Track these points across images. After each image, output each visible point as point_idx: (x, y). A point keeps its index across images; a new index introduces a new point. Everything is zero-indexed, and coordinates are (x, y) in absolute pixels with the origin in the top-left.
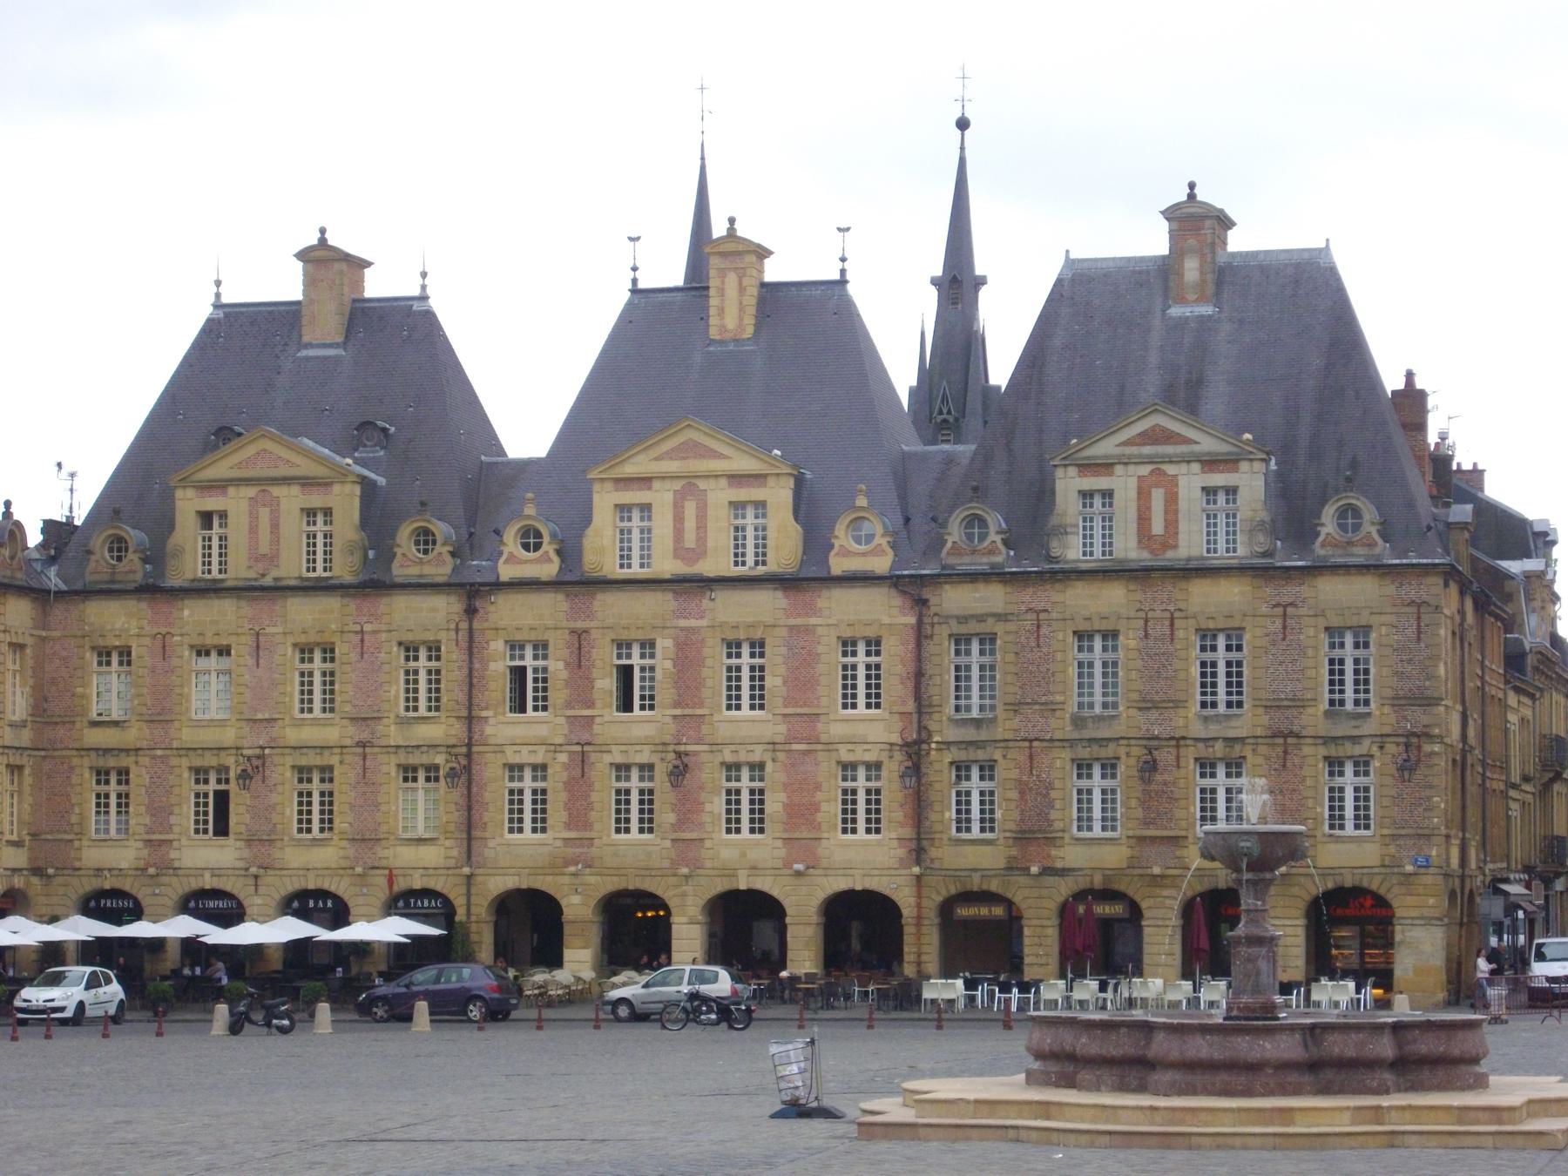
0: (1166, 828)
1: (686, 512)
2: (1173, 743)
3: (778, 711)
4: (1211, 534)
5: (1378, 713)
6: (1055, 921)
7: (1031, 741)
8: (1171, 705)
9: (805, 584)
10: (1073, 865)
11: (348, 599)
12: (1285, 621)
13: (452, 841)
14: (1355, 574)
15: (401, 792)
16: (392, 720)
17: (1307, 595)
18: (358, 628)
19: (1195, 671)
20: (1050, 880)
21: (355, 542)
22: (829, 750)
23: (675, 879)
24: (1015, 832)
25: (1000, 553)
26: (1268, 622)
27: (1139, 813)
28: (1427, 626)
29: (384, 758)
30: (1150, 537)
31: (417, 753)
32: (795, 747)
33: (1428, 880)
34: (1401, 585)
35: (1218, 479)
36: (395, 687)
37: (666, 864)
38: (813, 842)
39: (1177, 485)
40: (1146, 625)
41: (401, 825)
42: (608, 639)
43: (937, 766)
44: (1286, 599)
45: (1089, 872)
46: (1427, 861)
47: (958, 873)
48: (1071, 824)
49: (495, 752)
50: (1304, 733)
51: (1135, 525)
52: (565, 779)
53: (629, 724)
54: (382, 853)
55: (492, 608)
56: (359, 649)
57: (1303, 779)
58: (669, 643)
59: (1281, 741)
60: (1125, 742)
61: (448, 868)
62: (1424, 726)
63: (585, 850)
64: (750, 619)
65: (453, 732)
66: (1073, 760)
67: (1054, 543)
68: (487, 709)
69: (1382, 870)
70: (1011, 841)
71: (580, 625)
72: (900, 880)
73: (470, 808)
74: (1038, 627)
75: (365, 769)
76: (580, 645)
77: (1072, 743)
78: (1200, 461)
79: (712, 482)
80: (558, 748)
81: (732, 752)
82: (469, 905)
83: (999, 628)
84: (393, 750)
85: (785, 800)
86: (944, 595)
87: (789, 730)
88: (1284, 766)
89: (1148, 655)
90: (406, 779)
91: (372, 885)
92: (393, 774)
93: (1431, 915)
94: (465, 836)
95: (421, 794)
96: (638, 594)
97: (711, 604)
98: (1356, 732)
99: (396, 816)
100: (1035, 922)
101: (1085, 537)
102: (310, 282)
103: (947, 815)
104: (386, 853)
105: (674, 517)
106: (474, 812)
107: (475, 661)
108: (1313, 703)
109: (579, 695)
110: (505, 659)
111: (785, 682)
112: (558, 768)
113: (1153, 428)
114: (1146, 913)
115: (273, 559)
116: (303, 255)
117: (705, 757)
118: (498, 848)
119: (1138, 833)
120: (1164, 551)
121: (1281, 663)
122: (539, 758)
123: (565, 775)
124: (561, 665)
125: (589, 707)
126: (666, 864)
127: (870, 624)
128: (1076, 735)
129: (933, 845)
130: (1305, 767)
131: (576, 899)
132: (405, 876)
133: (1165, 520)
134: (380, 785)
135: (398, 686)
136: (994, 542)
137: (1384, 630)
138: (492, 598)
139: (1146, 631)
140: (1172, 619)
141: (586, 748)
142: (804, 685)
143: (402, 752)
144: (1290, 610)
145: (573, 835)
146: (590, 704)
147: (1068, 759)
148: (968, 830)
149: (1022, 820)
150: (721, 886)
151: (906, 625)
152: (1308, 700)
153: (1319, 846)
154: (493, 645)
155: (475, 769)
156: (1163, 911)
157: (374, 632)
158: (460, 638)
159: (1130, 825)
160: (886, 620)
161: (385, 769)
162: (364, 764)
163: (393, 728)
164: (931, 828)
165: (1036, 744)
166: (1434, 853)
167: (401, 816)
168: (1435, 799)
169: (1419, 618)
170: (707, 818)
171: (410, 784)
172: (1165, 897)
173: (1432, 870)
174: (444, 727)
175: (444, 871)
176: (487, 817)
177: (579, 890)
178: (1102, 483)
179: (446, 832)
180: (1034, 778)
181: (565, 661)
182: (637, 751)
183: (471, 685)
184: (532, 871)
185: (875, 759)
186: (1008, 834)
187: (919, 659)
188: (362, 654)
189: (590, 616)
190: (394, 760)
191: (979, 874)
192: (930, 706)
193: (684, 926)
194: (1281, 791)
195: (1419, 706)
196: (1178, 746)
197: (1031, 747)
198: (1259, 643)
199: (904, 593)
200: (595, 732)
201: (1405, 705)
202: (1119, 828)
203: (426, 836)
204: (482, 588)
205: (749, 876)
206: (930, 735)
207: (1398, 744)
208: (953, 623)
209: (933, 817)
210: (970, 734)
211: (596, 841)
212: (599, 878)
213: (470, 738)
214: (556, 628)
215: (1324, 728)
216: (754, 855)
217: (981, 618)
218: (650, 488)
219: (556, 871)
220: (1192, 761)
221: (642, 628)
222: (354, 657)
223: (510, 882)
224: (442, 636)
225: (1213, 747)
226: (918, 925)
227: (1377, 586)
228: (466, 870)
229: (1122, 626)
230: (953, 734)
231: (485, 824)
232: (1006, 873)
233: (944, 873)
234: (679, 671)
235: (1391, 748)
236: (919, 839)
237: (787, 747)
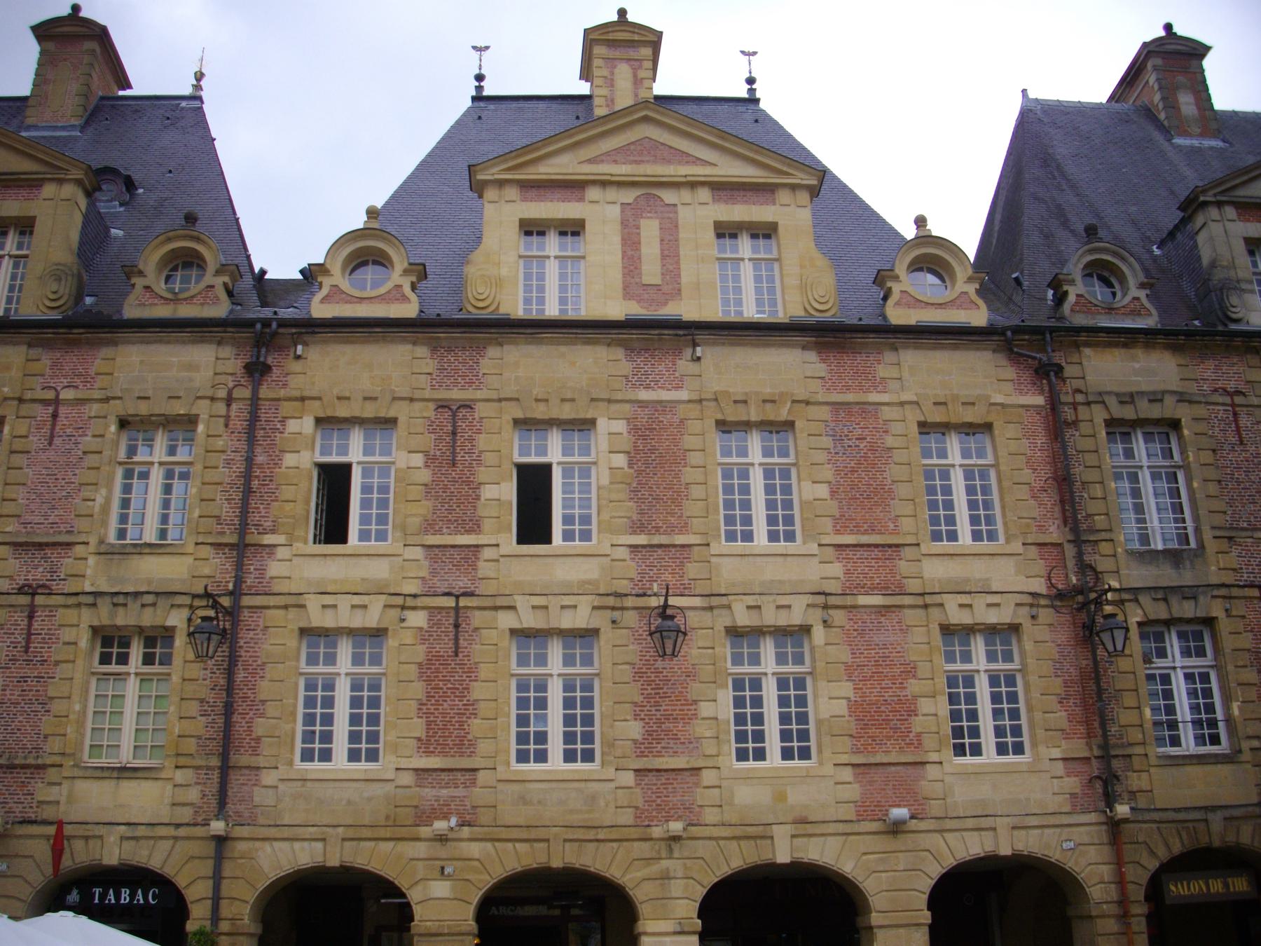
1: (643, 234)
3: (826, 540)
9: (859, 339)
11: (40, 350)
13: (190, 772)
15: (94, 682)
16: (92, 548)
18: (50, 395)
21: (64, 265)
22: (926, 606)
23: (646, 845)
29: (70, 615)
31: (134, 606)
32: (863, 600)
36: (104, 492)
37: (627, 817)
38: (910, 770)
41: (88, 742)
42: (507, 418)
47: (1181, 816)
49: (286, 607)
52: (421, 658)
53: (550, 560)
54: (43, 792)
55: (296, 366)
56: (46, 430)
58: (620, 426)
61: (178, 826)
63: (460, 792)
64: (768, 391)
65: (207, 571)
68: (273, 532)
71: (456, 394)
72: (1081, 834)
73: (229, 710)
74: (1235, 414)
75: (29, 634)
76: (454, 426)
79: (686, 195)
80: (410, 602)
81: (749, 607)
82: (216, 899)
84: (90, 599)
85: (851, 694)
87: (847, 572)
90: (105, 660)
91: (16, 856)
92: (84, 643)
94: (215, 762)
95: (132, 688)
96: (563, 349)
97: (693, 368)
99: (81, 723)
104: (53, 793)
105: (623, 239)
106: (236, 718)
107: (258, 450)
109: (450, 511)
110: (313, 450)
111: (833, 493)
112: (408, 638)
117: (693, 619)
118: (282, 787)
122: (371, 619)
123: (420, 653)
124: (418, 460)
125: (469, 532)
126: (627, 817)
127: (973, 404)
131: (441, 889)
132: (87, 838)
134: (57, 663)
135: (110, 492)
136: (1137, 299)
138: (300, 348)
141: (463, 602)
142: (869, 498)
143: (104, 606)
145: (434, 762)
146: (474, 526)
150: (736, 859)
154: (292, 426)
155: (244, 637)
158: (233, 414)
160: (999, 398)
161: (68, 634)
162: (30, 625)
163: (92, 560)
164: (1121, 737)
167: (89, 725)
170: (702, 729)
171: (114, 668)
174: (190, 560)
175: (171, 831)
176: (261, 727)
177: (448, 870)
179: (178, 755)
181: (426, 453)
182: (563, 607)
183: (248, 491)
184: (351, 833)
185: (1008, 621)
188: (52, 437)
189: (474, 380)
190: (87, 618)
193: (667, 939)
200: (480, 574)
203: (139, 763)
204: (281, 330)
205: (793, 836)
208: (1112, 402)
210: (1166, 575)
211: (481, 774)
212: (489, 845)
213: (239, 581)
214: (412, 400)
216: (797, 797)
218: (581, 199)
219: (403, 832)
221: (573, 400)
222: (35, 441)
223: (305, 855)
224: (202, 408)
228: (218, 827)
230: (1137, 575)
231: (258, 740)
233: (1156, 816)
234: (639, 472)
237: (849, 601)
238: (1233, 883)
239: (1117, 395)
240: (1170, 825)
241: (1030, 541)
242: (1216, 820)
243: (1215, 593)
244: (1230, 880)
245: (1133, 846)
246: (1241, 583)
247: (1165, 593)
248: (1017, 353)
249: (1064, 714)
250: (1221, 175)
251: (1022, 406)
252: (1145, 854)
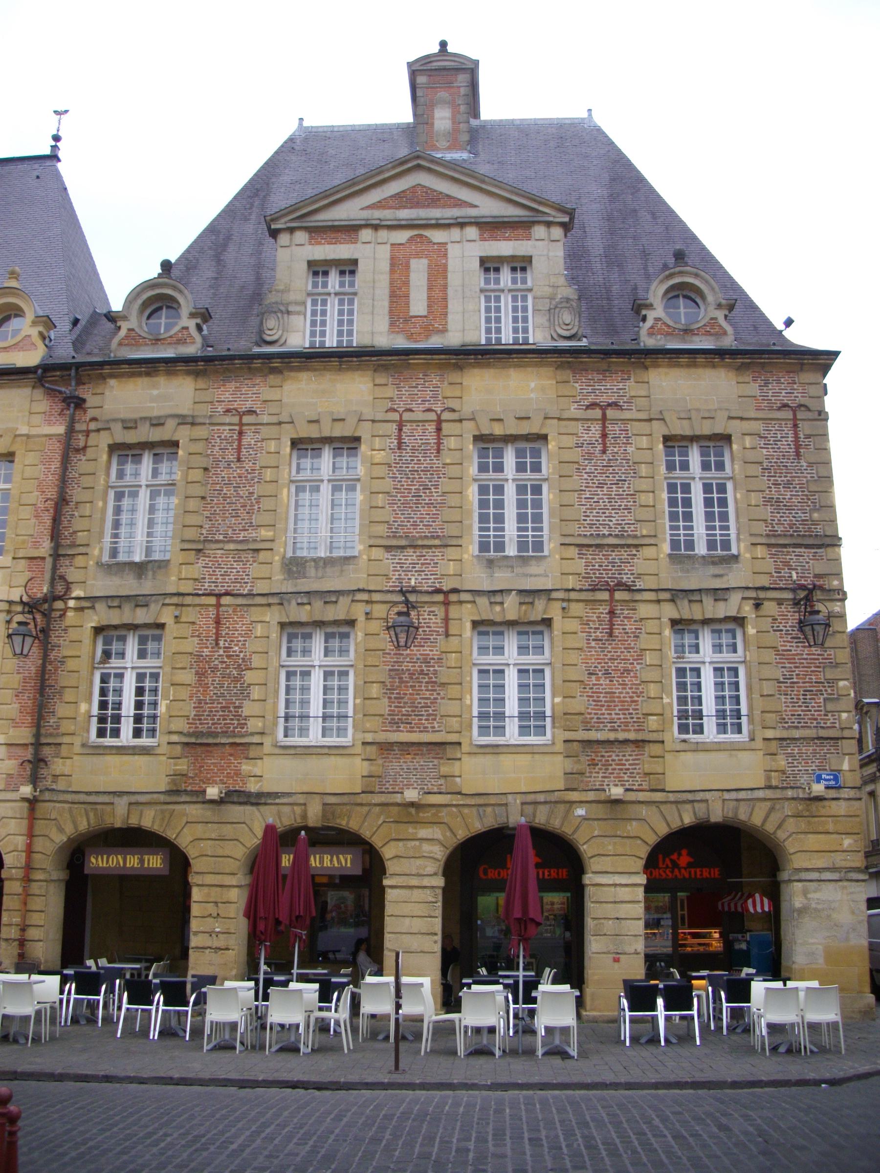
0: (425, 730)
2: (440, 598)
5: (748, 555)
6: (242, 879)
7: (219, 596)
8: (437, 542)
10: (275, 789)
12: (604, 427)
14: (704, 366)
17: (633, 394)
19: (472, 493)
20: (236, 811)
24: (189, 735)
25: (193, 343)
26: (579, 427)
27: (383, 706)
28: (808, 436)
30: (408, 319)
33: (841, 808)
34: (766, 384)
35: (504, 248)
39: (445, 255)
40: (400, 430)
43: (73, 634)
44: (604, 399)
45: (301, 799)
46: (836, 778)
48: (275, 724)
50: (639, 585)
51: (386, 304)
57: (640, 657)
60: (365, 596)
62: (816, 576)
66: (282, 625)
67: (271, 323)
69: (769, 794)
70: (179, 748)
74: (241, 433)
77: (281, 598)
83: (183, 435)
86: (107, 393)
88: (611, 634)
89: (401, 472)
93: (849, 864)
100: (209, 879)
103: (83, 707)
108: (652, 541)
114: (391, 867)
119: (382, 737)
121: (601, 485)
129: (57, 756)
130: (643, 636)
133: (429, 298)
137: (748, 441)
139: (400, 438)
140: (439, 422)
144: (610, 413)
147: (274, 623)
148: (116, 733)
149: (198, 717)
151: (49, 436)
152: (644, 536)
153: (668, 756)
156: (419, 862)
159: (368, 725)
160: (24, 430)
164: (58, 727)
165: (226, 600)
166: (846, 766)
168: (841, 684)
169: (795, 426)
172: (422, 840)
173: (845, 793)
178: (342, 251)
180: (221, 652)
186: (175, 738)
187: (63, 481)
191: (125, 800)
192: (74, 545)
194: (607, 673)
195: (807, 546)
196: (446, 604)
197: (218, 605)
198: (568, 456)
199: (51, 393)
201: (785, 546)
202: (350, 731)
206: (68, 589)
207: (780, 601)
208: (117, 428)
209: (62, 710)
210: (128, 585)
215: (670, 577)
217: (157, 423)
220: (468, 625)
225: (502, 603)
226: (27, 880)
227: (734, 383)
229: (364, 431)
232: (168, 799)
233: (69, 797)
235: (769, 607)
236: (38, 745)
238: (149, 860)
239: (123, 421)
240: (81, 806)
241: (21, 555)
242: (121, 805)
243: (167, 601)
244: (146, 857)
245: (46, 822)
246: (200, 592)
248: (48, 388)
249: (17, 705)
250: (294, 202)
251: (46, 436)
252: (54, 829)
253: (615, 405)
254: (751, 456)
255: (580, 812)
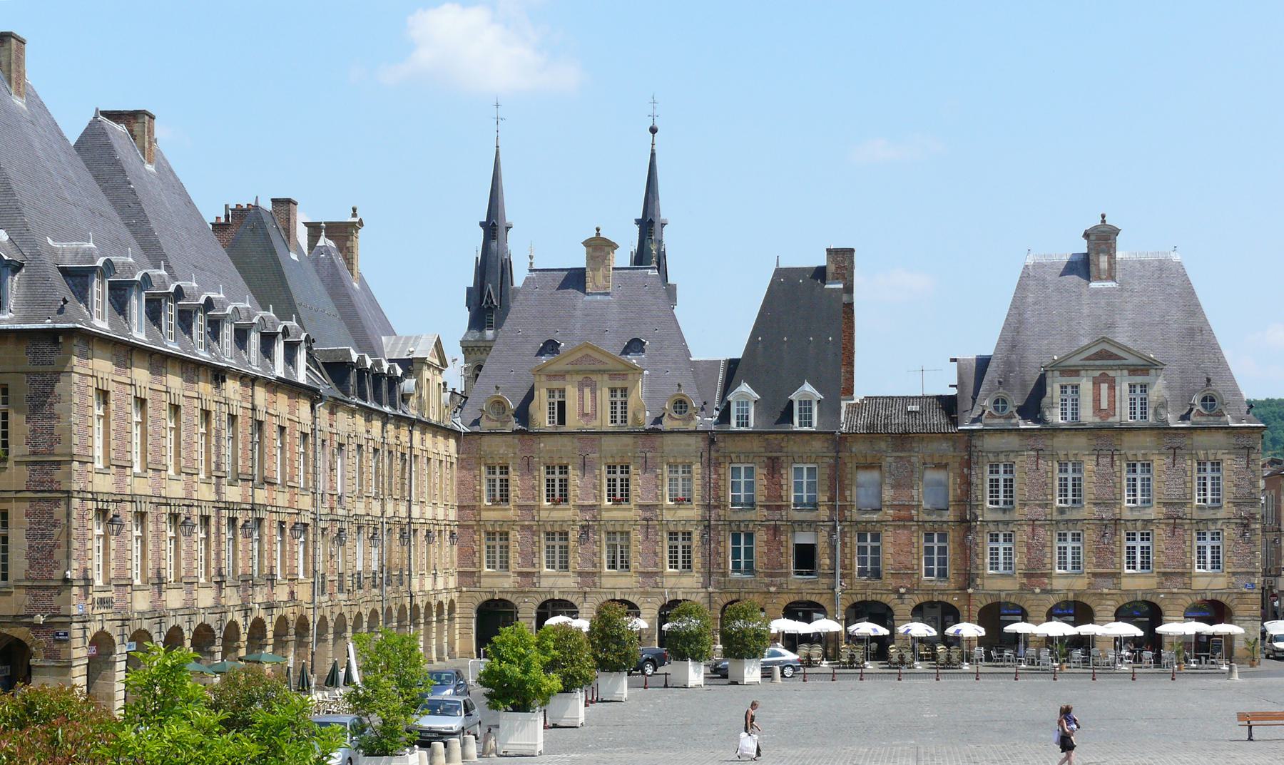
2: (1113, 522)
4: (1133, 409)
7: (1034, 521)
30: (1100, 410)
45: (1065, 592)
59: (1173, 521)
70: (1022, 576)
78: (1127, 369)
98: (1213, 517)
101: (1062, 409)
102: (590, 258)
113: (1101, 351)
115: (594, 415)
116: (587, 243)
120: (1108, 418)
128: (1059, 518)
137: (1229, 462)
140: (1113, 455)
157: (653, 457)
178: (1074, 381)
196: (1116, 524)
210: (1000, 517)
230: (989, 517)
247: (997, 522)
253: (1179, 448)
254: (1230, 468)
255: (1162, 596)
